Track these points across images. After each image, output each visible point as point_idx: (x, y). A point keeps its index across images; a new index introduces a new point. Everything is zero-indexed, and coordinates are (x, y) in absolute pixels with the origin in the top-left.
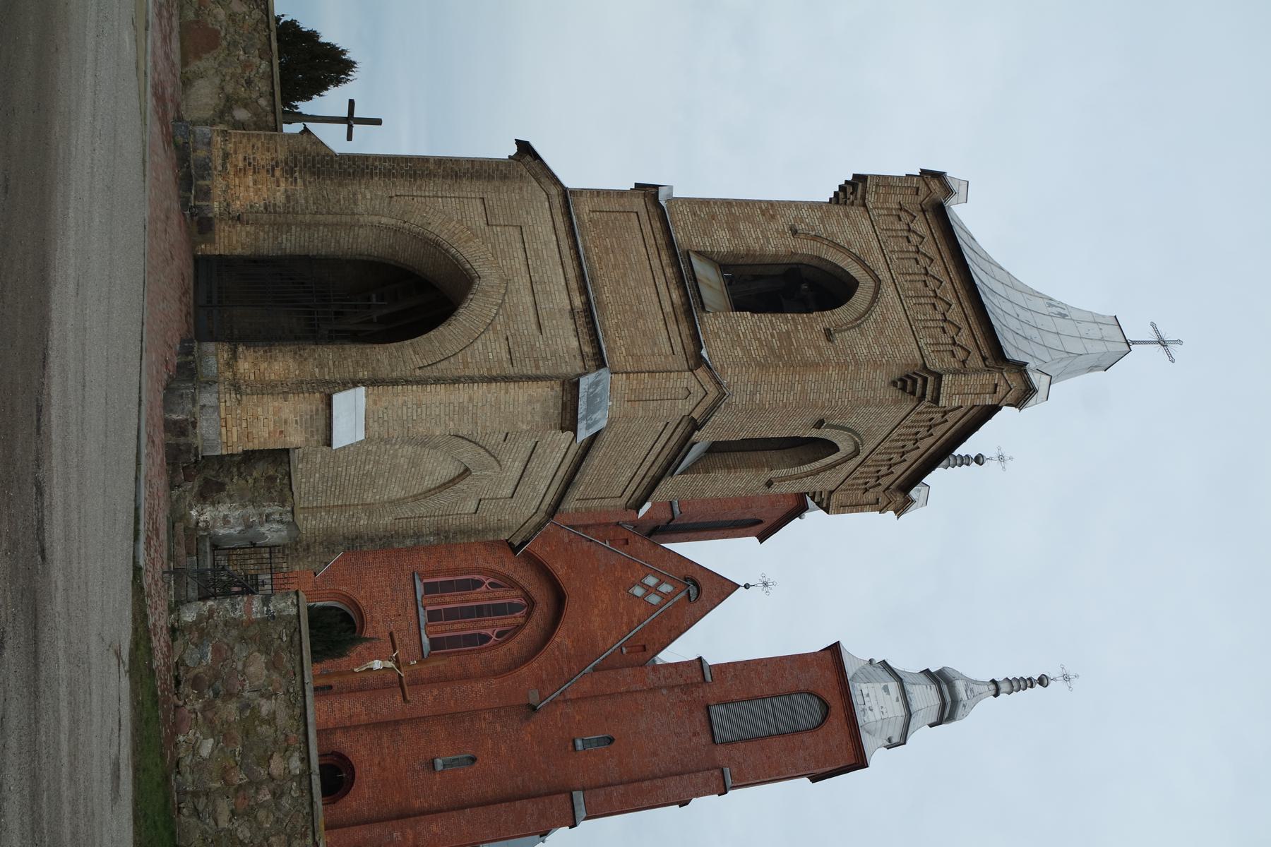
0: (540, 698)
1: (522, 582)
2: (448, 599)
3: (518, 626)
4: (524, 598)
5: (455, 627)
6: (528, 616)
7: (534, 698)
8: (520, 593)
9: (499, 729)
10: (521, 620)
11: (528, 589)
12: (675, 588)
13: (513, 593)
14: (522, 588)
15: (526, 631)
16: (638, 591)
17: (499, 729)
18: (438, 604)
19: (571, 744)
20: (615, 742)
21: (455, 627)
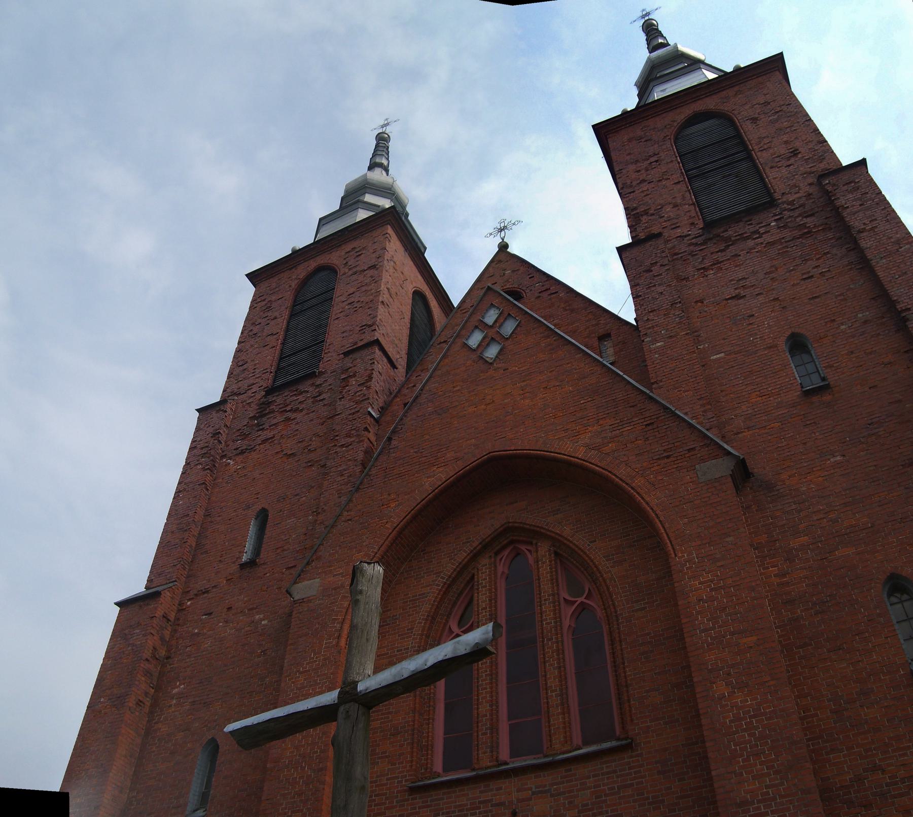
0: (716, 457)
1: (462, 556)
2: (484, 708)
3: (556, 554)
4: (496, 554)
5: (553, 682)
6: (533, 535)
7: (720, 468)
8: (485, 561)
9: (804, 539)
10: (544, 549)
11: (475, 545)
12: (492, 305)
13: (483, 576)
14: (475, 556)
15: (567, 531)
16: (492, 352)
17: (804, 539)
18: (494, 729)
19: (815, 399)
20: (797, 330)
21: (553, 682)
